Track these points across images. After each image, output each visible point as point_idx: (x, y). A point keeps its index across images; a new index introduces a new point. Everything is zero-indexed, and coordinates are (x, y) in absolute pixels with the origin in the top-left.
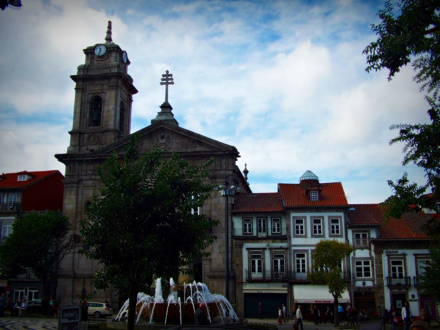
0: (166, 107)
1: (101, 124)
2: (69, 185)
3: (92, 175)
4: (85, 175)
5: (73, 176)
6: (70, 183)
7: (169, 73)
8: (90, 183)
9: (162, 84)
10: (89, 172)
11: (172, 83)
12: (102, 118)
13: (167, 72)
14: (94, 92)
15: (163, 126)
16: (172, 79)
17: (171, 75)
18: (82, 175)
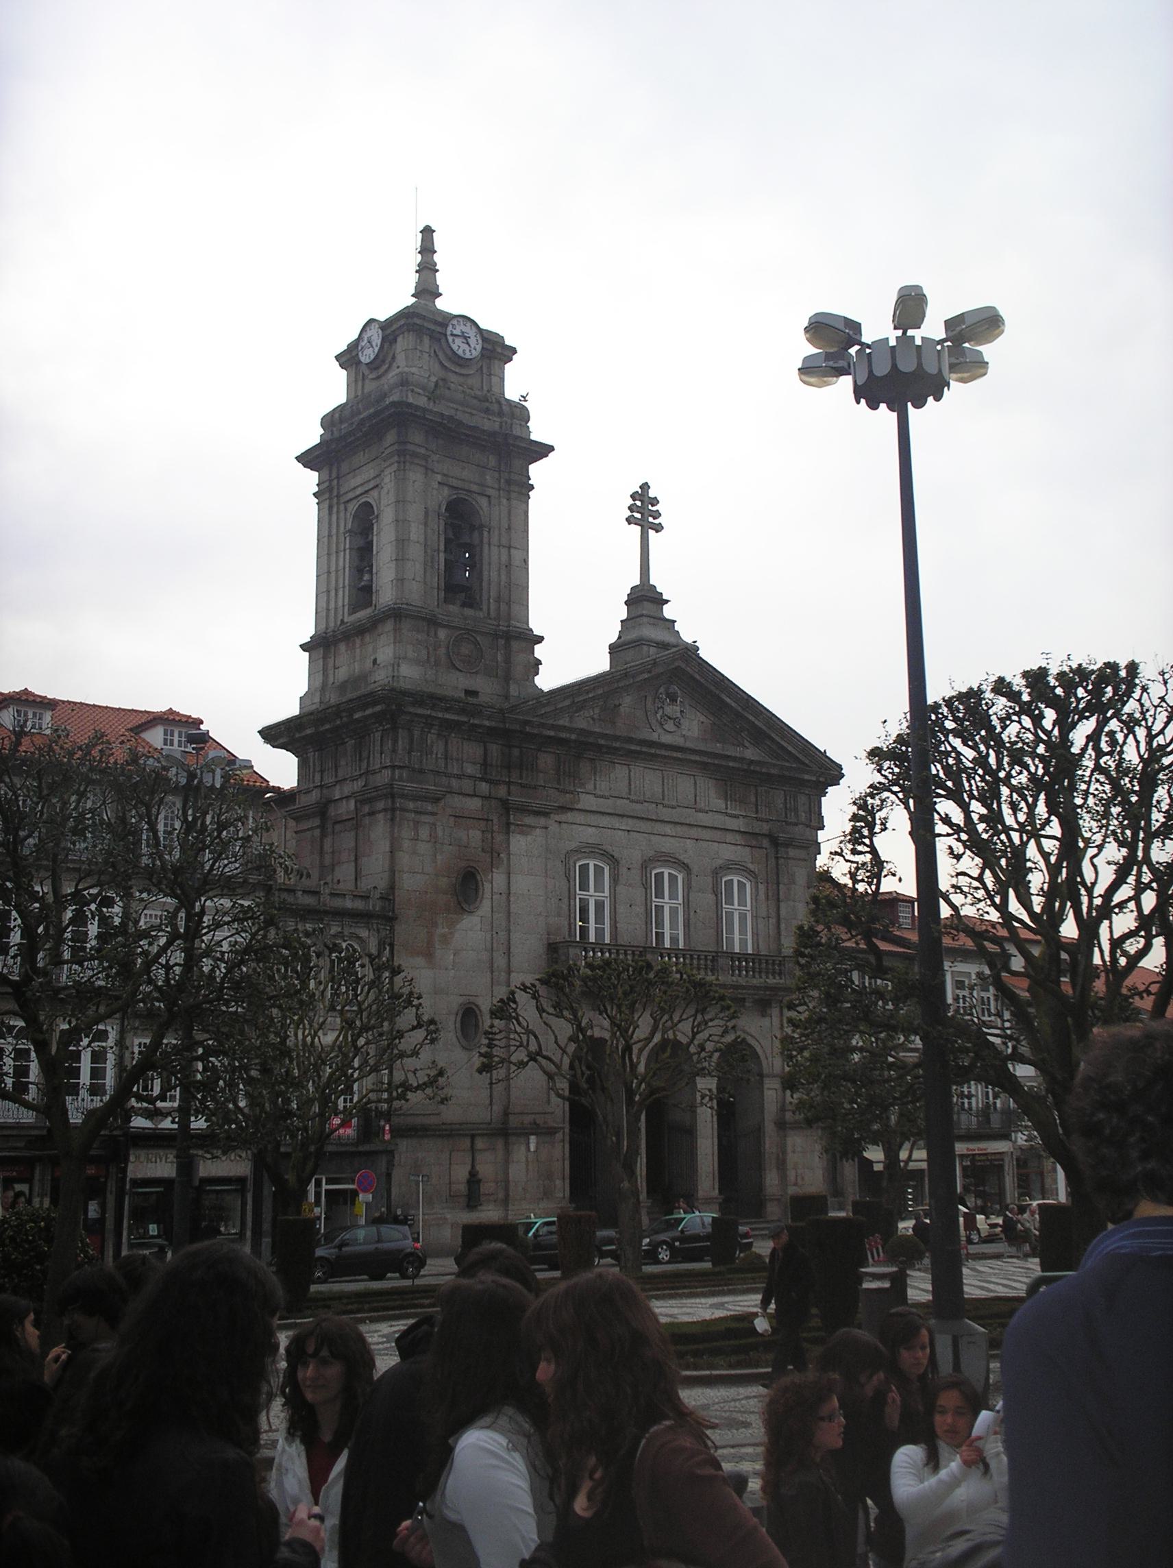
0: (645, 600)
1: (485, 607)
2: (411, 805)
3: (482, 779)
4: (459, 777)
5: (421, 771)
6: (415, 798)
7: (652, 494)
8: (474, 804)
9: (629, 521)
10: (469, 769)
11: (658, 528)
12: (485, 584)
13: (645, 487)
14: (459, 484)
15: (683, 666)
16: (657, 515)
17: (655, 501)
18: (449, 776)
